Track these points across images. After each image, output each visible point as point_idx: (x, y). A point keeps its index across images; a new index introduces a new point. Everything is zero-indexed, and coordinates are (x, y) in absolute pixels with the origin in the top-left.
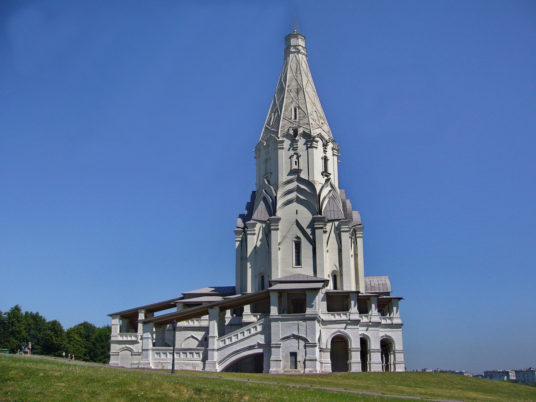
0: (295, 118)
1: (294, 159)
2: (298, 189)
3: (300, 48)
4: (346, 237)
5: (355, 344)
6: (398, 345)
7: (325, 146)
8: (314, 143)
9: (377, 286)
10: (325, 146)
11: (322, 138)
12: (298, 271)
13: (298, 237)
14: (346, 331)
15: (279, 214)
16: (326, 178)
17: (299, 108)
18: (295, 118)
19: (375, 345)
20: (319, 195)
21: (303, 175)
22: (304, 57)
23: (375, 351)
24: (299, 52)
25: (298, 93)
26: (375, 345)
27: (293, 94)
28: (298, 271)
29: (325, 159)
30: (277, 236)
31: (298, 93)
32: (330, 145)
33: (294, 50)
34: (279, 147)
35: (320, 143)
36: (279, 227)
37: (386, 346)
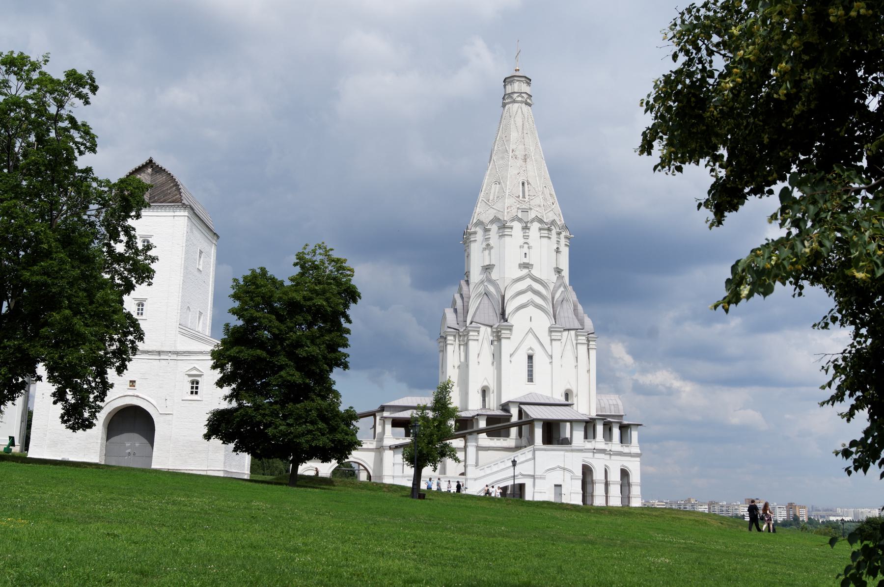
0: (524, 197)
1: (525, 250)
4: (583, 349)
5: (598, 475)
6: (635, 478)
9: (607, 406)
10: (559, 234)
12: (530, 388)
13: (531, 349)
14: (590, 461)
15: (512, 320)
17: (528, 183)
18: (524, 197)
19: (615, 476)
20: (553, 298)
21: (535, 272)
23: (615, 483)
25: (525, 160)
27: (520, 162)
28: (530, 388)
29: (558, 251)
31: (525, 160)
33: (520, 99)
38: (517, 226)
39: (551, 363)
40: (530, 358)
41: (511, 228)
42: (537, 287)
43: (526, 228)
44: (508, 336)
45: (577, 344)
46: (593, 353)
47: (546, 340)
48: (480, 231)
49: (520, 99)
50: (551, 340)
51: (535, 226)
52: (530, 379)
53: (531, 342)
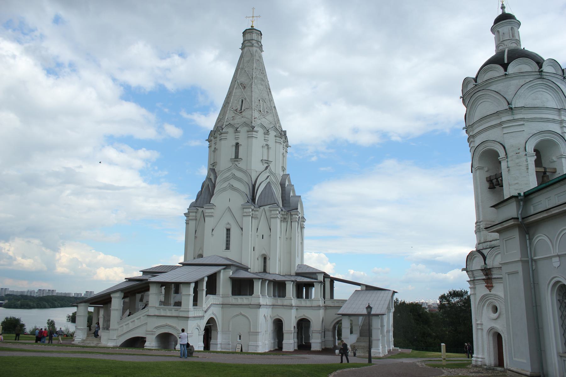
0: (241, 110)
3: (254, 42)
7: (267, 133)
8: (254, 133)
11: (263, 126)
13: (228, 223)
19: (290, 326)
22: (258, 50)
24: (252, 46)
26: (290, 326)
32: (272, 133)
35: (261, 131)
37: (303, 325)
38: (231, 130)
40: (228, 230)
42: (239, 174)
43: (236, 131)
47: (237, 215)
49: (249, 44)
51: (243, 130)
52: (228, 248)
53: (227, 219)
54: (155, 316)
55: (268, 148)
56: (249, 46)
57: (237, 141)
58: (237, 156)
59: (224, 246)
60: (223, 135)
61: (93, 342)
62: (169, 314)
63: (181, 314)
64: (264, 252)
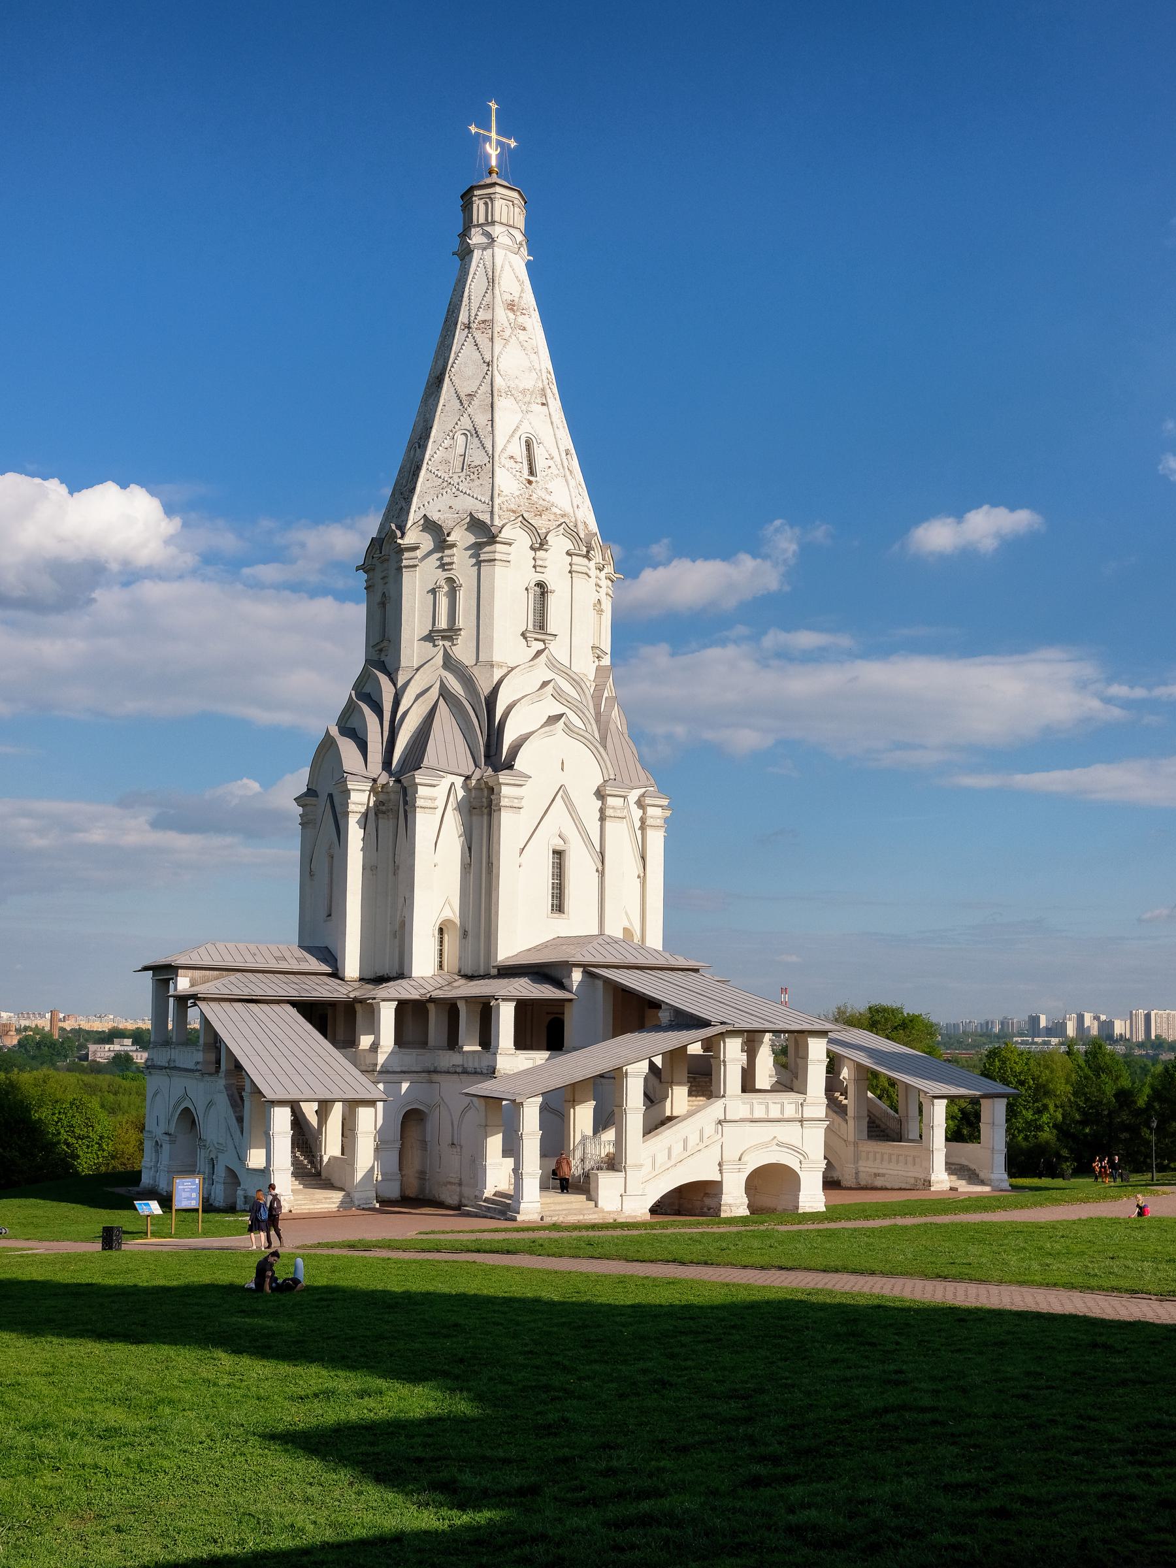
2: (559, 695)
16: (597, 663)
30: (511, 827)
34: (497, 556)
36: (523, 803)
39: (602, 873)
40: (559, 854)
41: (510, 544)
43: (540, 544)
44: (516, 803)
45: (643, 828)
46: (656, 841)
48: (427, 542)
50: (602, 819)
52: (559, 906)
54: (742, 1120)
55: (600, 612)
56: (507, 248)
57: (540, 577)
58: (541, 624)
59: (547, 901)
60: (498, 547)
61: (569, 1208)
62: (775, 1113)
63: (808, 1112)
64: (627, 925)
